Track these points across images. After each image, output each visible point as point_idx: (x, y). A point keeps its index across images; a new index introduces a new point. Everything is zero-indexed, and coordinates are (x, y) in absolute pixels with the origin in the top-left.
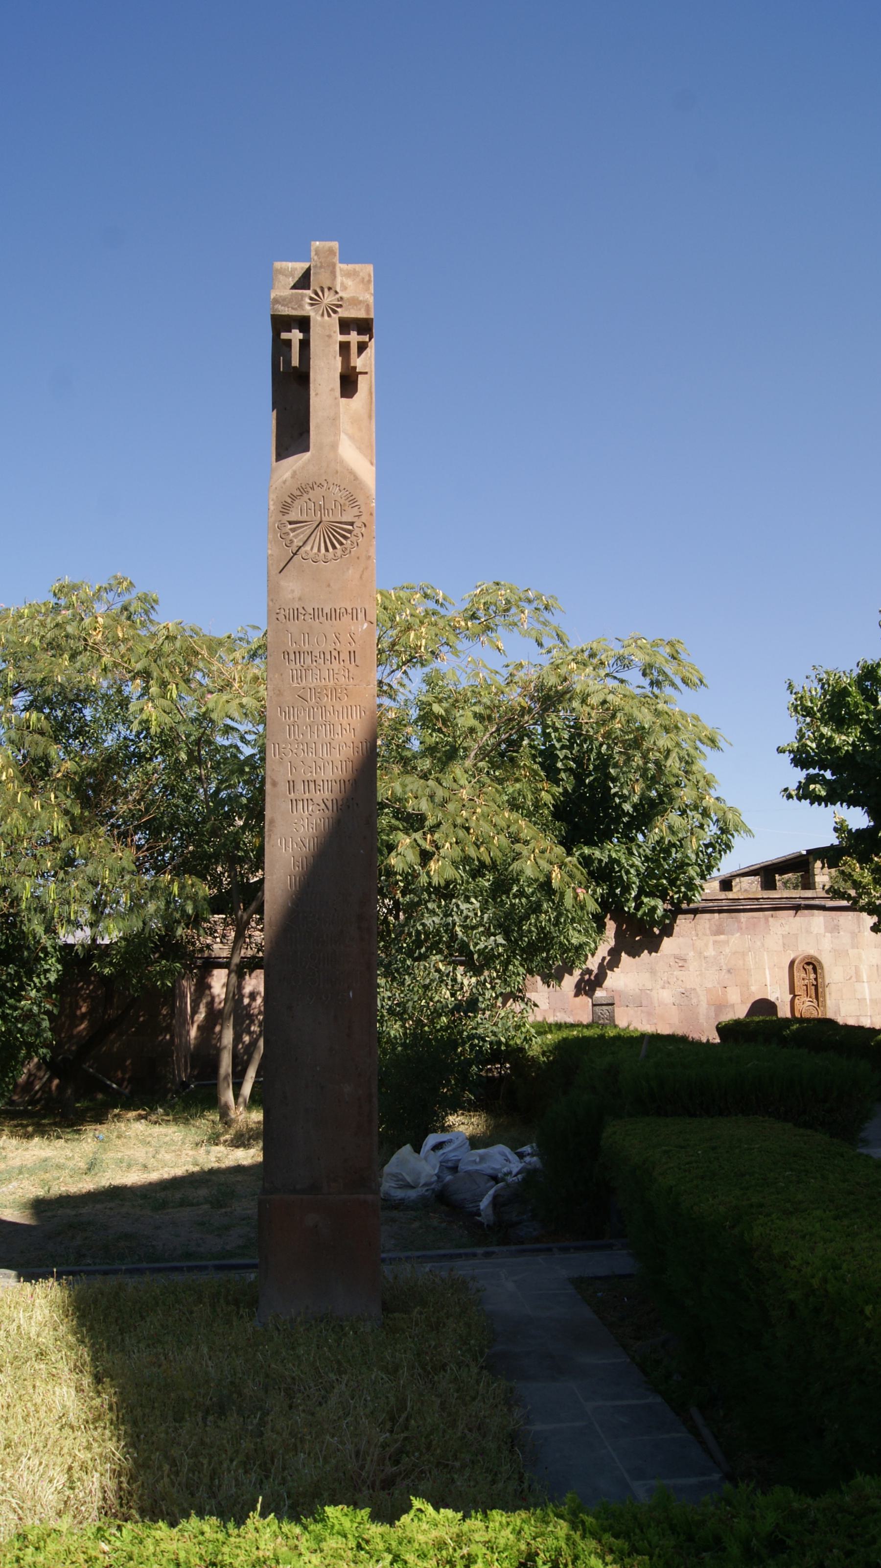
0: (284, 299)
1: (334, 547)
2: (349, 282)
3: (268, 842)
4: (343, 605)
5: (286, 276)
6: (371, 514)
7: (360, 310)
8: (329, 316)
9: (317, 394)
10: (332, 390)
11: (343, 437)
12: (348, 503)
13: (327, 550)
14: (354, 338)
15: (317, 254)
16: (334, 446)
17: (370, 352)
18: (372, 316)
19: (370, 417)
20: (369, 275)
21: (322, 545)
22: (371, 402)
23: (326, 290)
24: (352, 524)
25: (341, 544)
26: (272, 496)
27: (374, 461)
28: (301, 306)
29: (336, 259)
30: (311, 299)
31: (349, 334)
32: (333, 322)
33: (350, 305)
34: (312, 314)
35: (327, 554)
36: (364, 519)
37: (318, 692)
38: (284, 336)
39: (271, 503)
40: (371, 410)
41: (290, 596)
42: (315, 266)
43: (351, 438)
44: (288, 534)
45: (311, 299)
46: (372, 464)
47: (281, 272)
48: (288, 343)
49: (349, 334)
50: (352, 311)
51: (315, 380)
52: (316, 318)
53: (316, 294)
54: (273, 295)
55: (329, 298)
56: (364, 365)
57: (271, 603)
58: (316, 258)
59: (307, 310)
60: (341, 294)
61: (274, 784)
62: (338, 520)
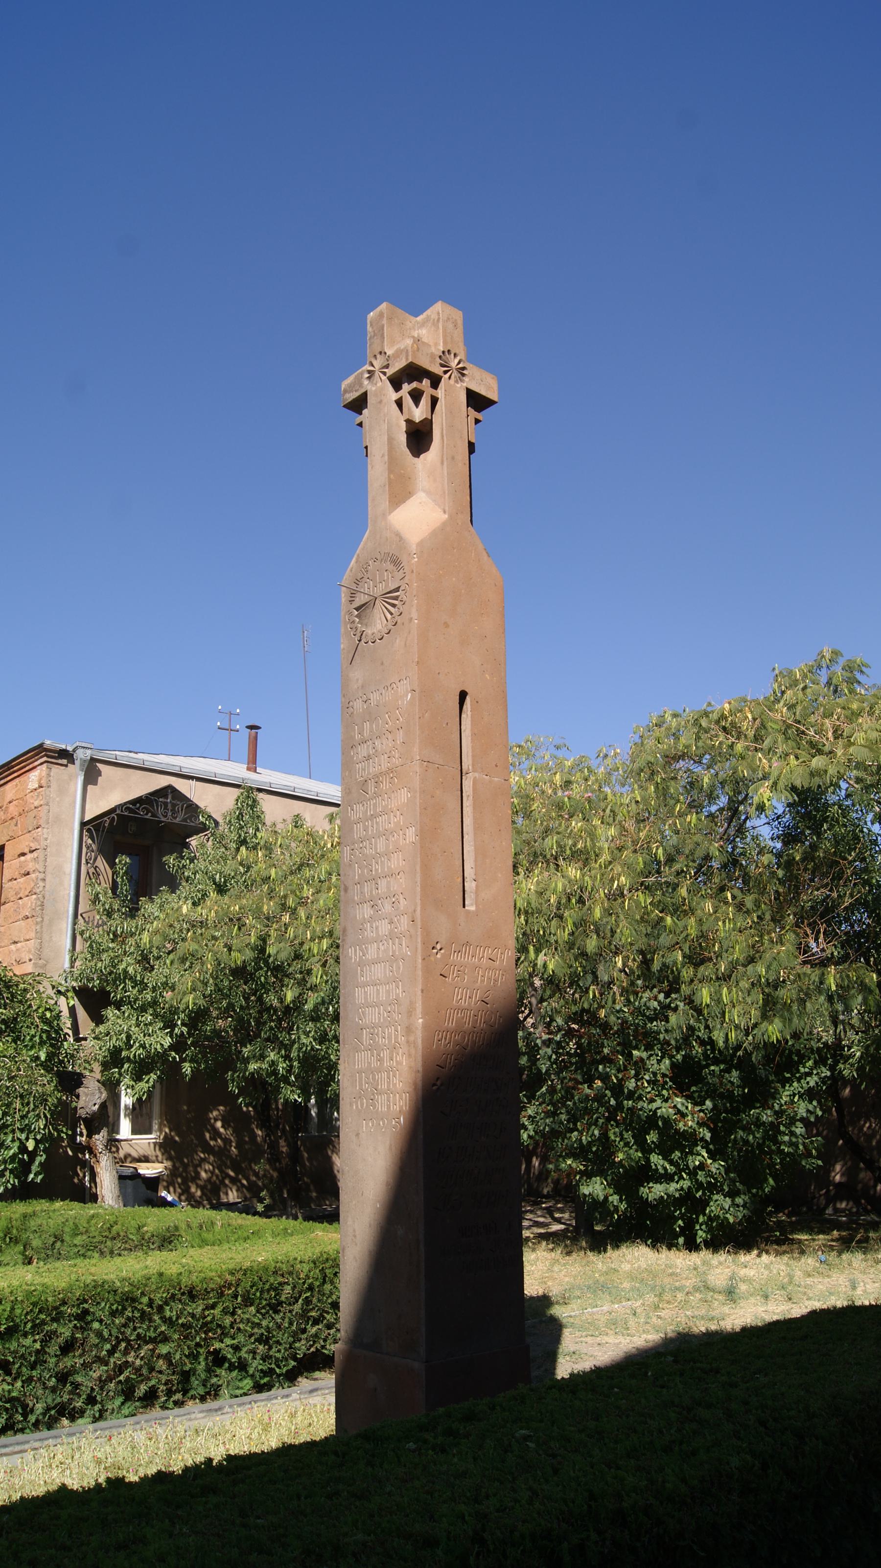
15: (371, 325)
18: (410, 360)
19: (442, 463)
23: (378, 356)
24: (397, 590)
27: (447, 508)
28: (361, 385)
36: (406, 580)
43: (428, 493)
46: (445, 512)
62: (388, 590)
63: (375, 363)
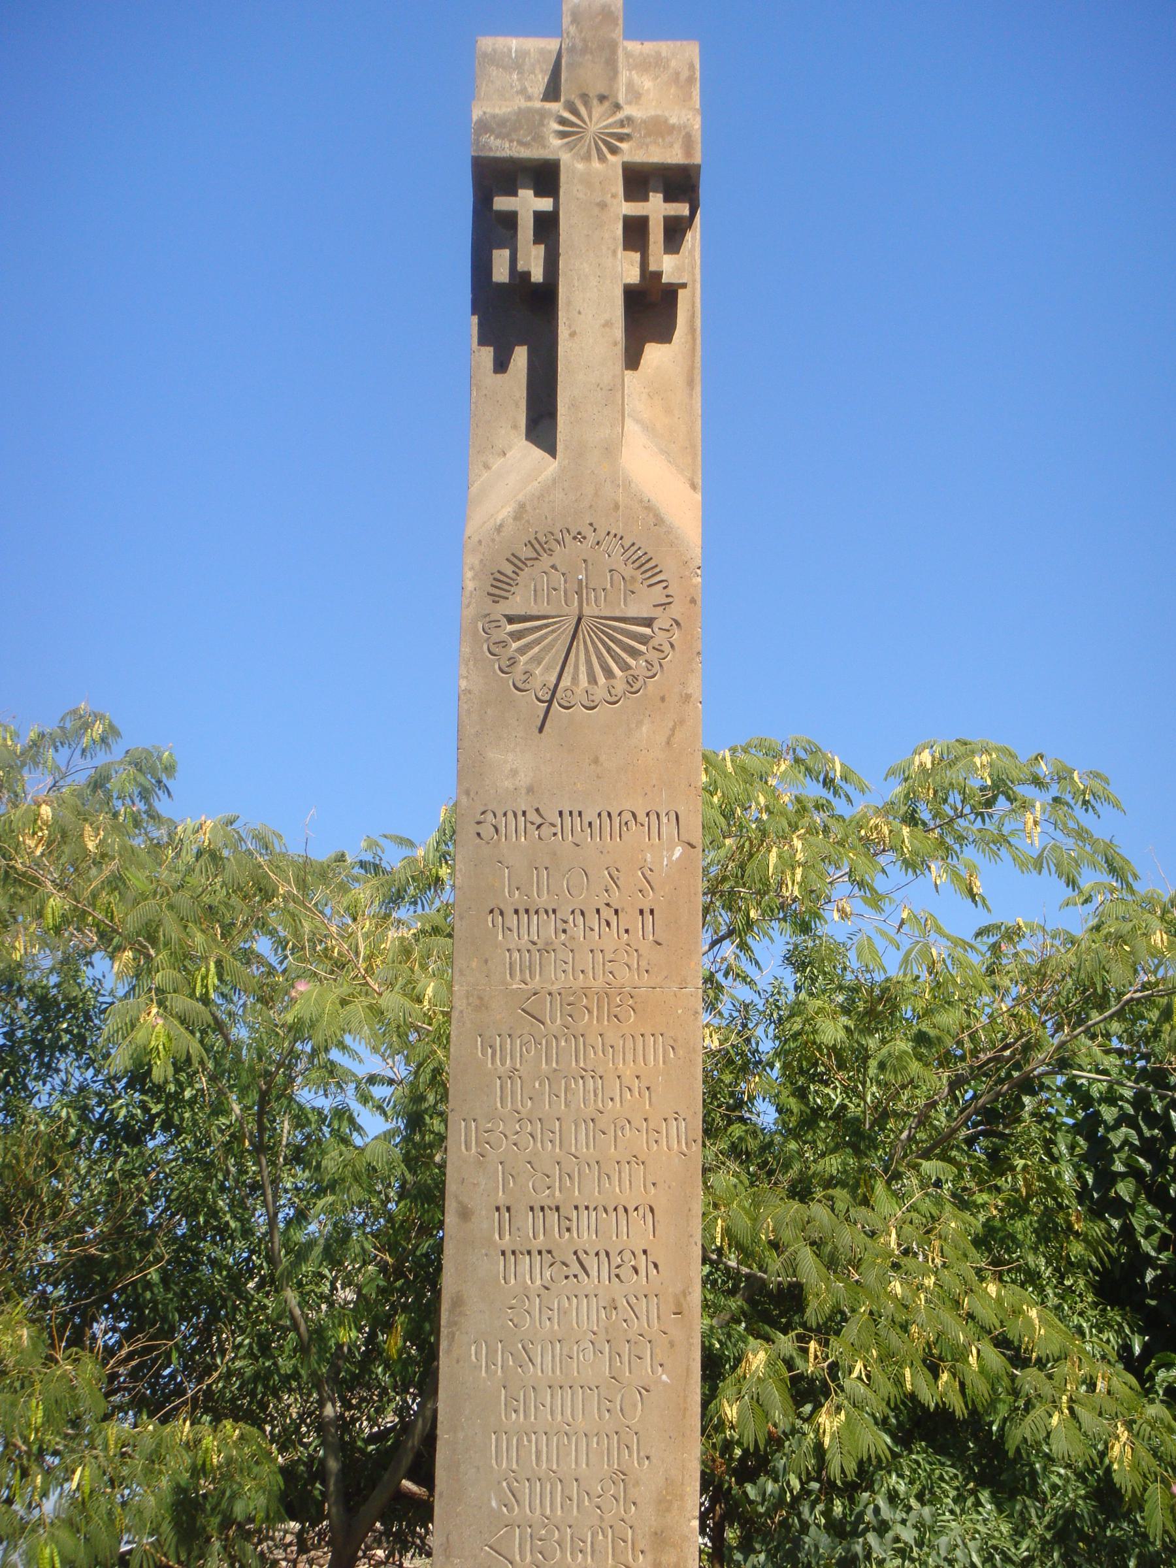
0: (502, 122)
1: (609, 674)
2: (646, 83)
3: (449, 1351)
4: (627, 805)
5: (504, 68)
6: (693, 601)
7: (671, 146)
8: (602, 158)
9: (573, 334)
10: (608, 324)
11: (631, 426)
12: (640, 578)
13: (593, 680)
14: (656, 208)
15: (575, 20)
16: (611, 450)
17: (693, 239)
18: (697, 159)
19: (691, 383)
20: (691, 66)
21: (583, 669)
22: (693, 349)
24: (648, 622)
25: (625, 667)
26: (472, 560)
27: (699, 481)
28: (539, 139)
29: (619, 30)
30: (563, 121)
31: (646, 199)
32: (611, 171)
33: (648, 134)
34: (565, 158)
35: (592, 689)
36: (675, 611)
37: (571, 1002)
38: (502, 203)
39: (469, 574)
40: (692, 368)
41: (508, 784)
42: (572, 50)
43: (648, 428)
44: (503, 644)
45: (563, 121)
46: (694, 487)
47: (494, 59)
48: (510, 220)
49: (646, 199)
50: (652, 148)
51: (569, 303)
52: (572, 167)
53: (575, 112)
54: (476, 114)
55: (598, 121)
56: (679, 269)
57: (464, 800)
58: (573, 30)
59: (553, 147)
60: (628, 111)
61: (465, 1214)
62: (618, 614)
63: (583, 111)
